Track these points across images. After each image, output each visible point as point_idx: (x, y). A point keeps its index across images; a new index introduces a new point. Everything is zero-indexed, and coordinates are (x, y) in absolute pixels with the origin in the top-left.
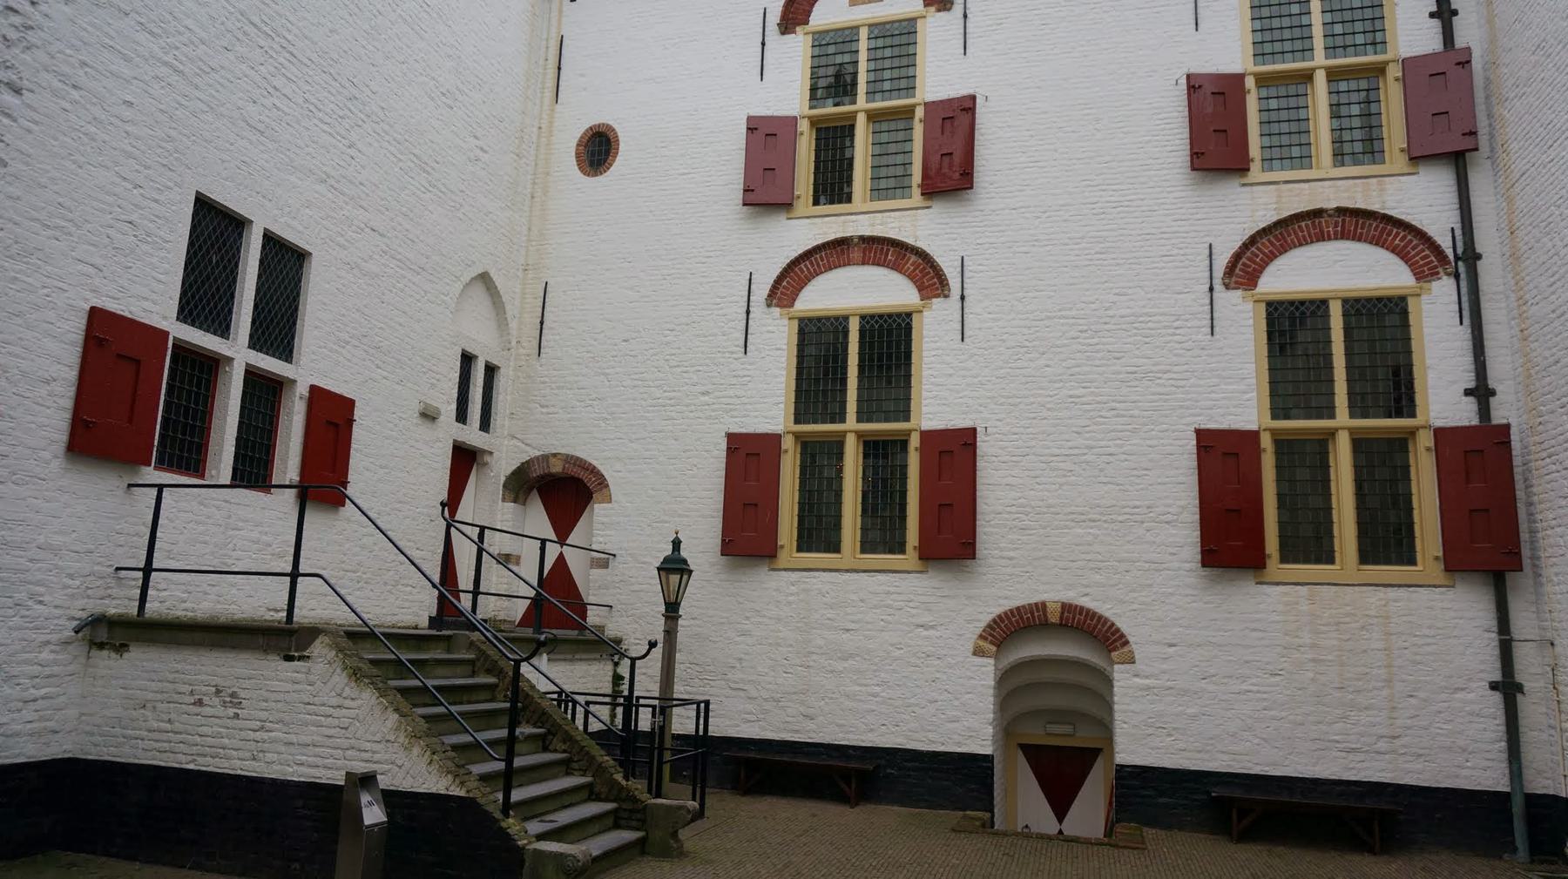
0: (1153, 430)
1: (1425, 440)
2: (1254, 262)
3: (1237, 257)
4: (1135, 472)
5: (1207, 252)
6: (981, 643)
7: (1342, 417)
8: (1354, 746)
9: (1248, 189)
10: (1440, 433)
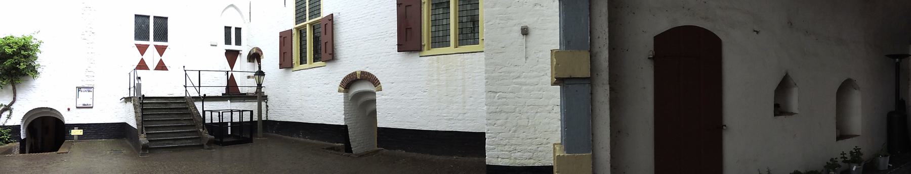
4: (382, 19)
6: (340, 88)
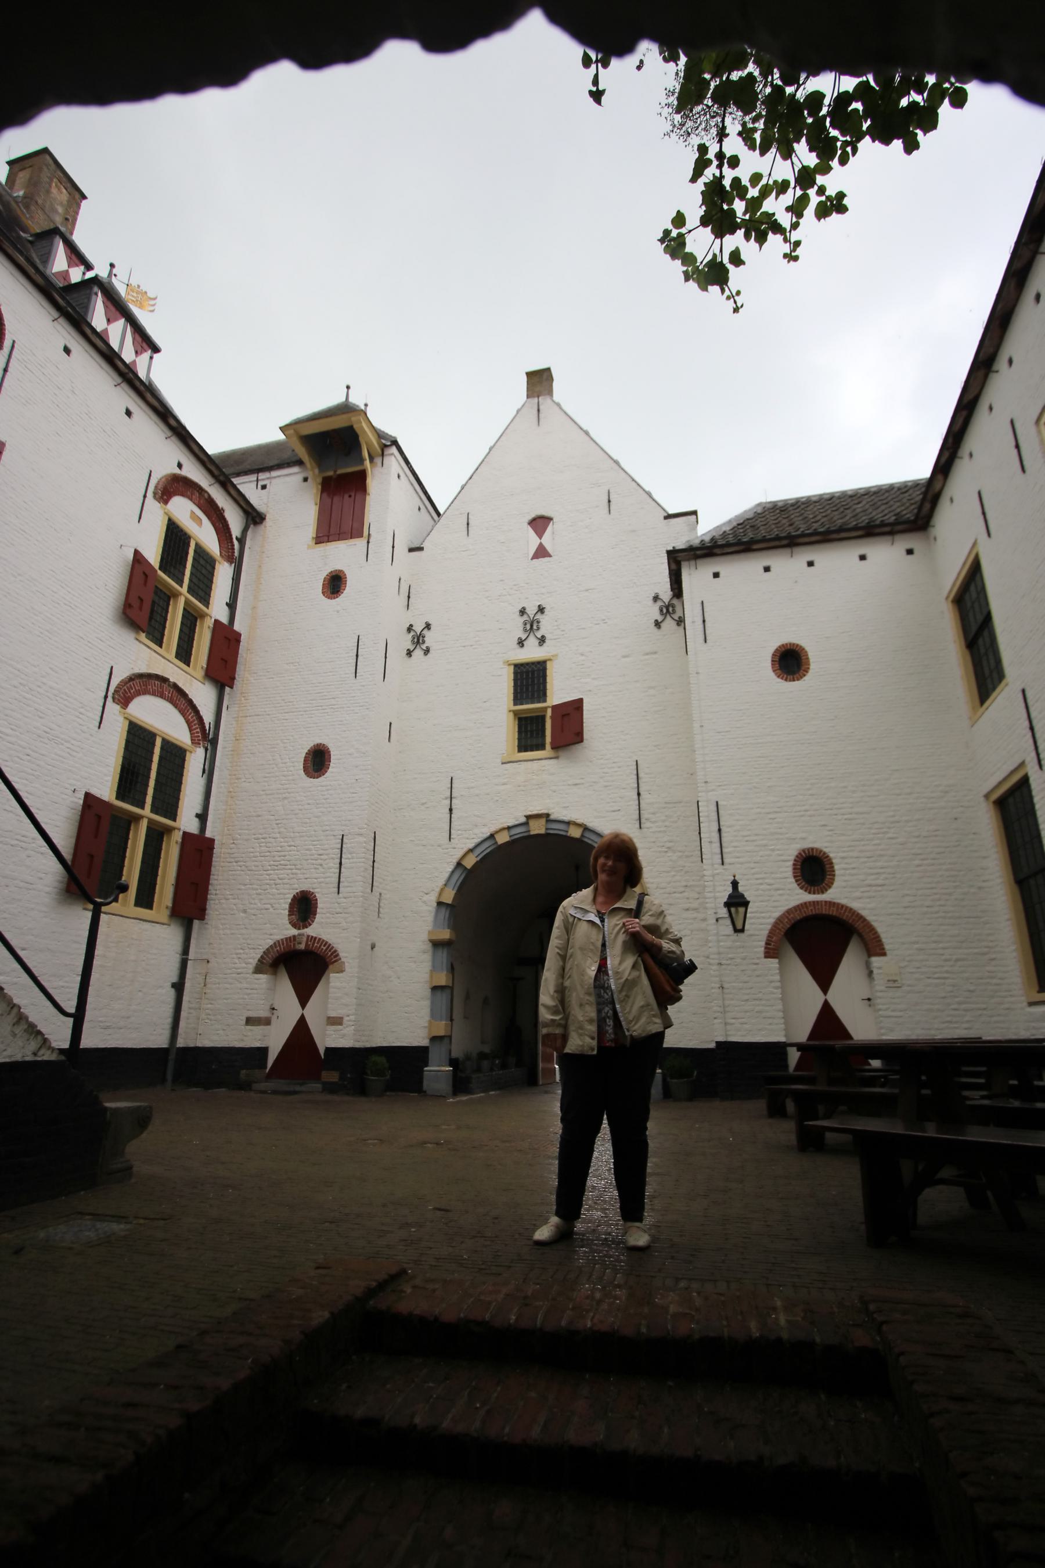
0: (49, 781)
1: (177, 837)
2: (130, 691)
3: (124, 683)
5: (109, 670)
7: (147, 811)
8: (108, 1024)
9: (137, 643)
10: (186, 835)
